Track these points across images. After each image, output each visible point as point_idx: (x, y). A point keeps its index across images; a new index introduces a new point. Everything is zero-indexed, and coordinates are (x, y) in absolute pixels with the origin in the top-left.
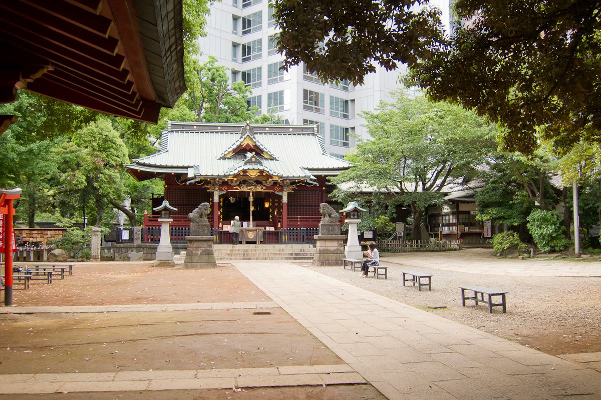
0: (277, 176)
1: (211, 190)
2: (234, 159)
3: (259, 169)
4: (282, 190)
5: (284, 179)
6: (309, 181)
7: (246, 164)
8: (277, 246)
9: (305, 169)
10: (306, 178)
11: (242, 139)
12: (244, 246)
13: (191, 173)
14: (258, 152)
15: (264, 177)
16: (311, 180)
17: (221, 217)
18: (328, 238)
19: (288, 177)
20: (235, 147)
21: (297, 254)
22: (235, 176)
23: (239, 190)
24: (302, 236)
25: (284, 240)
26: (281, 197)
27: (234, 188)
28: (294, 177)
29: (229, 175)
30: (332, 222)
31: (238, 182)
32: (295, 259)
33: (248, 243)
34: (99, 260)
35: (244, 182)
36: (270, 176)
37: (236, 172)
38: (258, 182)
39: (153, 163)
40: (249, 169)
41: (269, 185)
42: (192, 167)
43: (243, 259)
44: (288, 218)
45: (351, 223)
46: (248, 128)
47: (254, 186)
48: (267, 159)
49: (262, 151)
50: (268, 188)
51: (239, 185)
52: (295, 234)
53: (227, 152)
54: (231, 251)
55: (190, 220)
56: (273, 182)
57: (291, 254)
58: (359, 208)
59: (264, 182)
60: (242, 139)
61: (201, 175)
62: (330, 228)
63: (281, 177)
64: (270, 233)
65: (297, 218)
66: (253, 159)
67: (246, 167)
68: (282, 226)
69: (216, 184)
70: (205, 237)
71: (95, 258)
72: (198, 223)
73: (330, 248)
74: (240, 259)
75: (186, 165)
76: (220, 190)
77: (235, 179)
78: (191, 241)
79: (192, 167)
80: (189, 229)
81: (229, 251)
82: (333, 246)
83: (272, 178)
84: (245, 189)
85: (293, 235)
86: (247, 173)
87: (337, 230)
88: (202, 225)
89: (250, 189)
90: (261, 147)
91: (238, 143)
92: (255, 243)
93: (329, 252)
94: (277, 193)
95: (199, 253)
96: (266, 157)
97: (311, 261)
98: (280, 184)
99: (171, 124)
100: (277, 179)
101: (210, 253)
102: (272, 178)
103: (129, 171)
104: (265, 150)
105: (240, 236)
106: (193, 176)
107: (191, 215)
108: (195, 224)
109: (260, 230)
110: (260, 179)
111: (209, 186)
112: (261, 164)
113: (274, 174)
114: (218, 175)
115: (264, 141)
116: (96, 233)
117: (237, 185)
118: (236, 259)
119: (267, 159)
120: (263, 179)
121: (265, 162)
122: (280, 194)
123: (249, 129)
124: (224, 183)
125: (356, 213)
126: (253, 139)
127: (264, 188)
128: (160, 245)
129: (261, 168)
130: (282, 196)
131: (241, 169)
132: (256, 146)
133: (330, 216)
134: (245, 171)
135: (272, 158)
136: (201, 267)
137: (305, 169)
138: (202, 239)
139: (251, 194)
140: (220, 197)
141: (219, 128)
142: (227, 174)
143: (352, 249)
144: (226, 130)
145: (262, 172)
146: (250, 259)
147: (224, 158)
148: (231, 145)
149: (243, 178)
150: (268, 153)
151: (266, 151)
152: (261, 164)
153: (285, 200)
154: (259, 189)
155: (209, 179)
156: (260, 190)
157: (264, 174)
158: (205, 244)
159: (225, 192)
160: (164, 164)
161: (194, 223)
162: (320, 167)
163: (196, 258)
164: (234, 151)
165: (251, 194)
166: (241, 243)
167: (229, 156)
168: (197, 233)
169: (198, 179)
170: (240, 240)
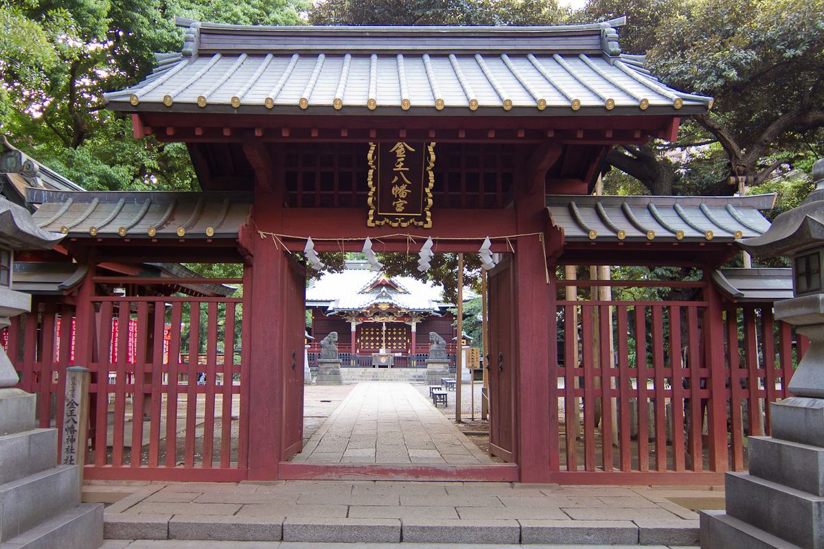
4: (411, 321)
7: (377, 298)
8: (404, 370)
12: (377, 370)
13: (331, 306)
16: (435, 311)
20: (372, 282)
21: (419, 377)
22: (368, 309)
29: (363, 308)
32: (417, 380)
33: (380, 367)
35: (377, 314)
36: (399, 309)
37: (369, 305)
38: (390, 314)
43: (372, 380)
50: (398, 319)
52: (422, 359)
54: (363, 373)
55: (321, 346)
57: (415, 376)
63: (408, 309)
64: (398, 358)
66: (384, 294)
67: (377, 301)
70: (333, 360)
73: (437, 370)
75: (328, 299)
76: (357, 320)
78: (322, 363)
82: (439, 368)
84: (378, 319)
91: (375, 279)
95: (328, 373)
96: (401, 291)
98: (408, 315)
101: (337, 373)
104: (399, 285)
105: (374, 361)
107: (322, 342)
112: (391, 298)
122: (409, 324)
124: (360, 314)
129: (390, 301)
131: (373, 302)
133: (437, 343)
134: (376, 305)
136: (329, 385)
139: (384, 324)
141: (362, 265)
145: (391, 305)
146: (377, 380)
147: (362, 292)
152: (391, 298)
153: (414, 329)
154: (390, 319)
156: (392, 321)
157: (394, 307)
158: (333, 365)
163: (325, 378)
164: (371, 286)
165: (384, 324)
166: (374, 367)
167: (367, 290)
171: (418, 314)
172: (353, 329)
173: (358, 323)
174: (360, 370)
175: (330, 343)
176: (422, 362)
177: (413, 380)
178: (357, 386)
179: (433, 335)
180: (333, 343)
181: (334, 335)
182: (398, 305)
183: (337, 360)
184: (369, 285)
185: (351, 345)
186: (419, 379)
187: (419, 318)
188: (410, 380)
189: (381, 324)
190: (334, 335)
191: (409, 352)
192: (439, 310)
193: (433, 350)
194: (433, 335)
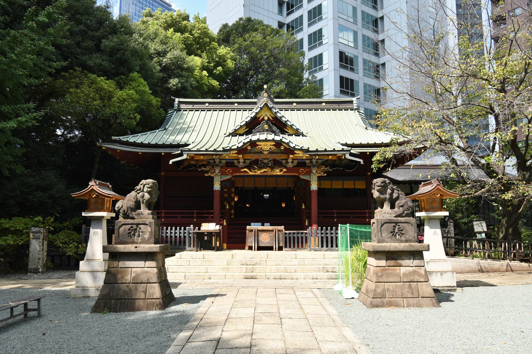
4: (309, 173)
6: (348, 156)
10: (345, 153)
17: (233, 212)
19: (317, 151)
27: (243, 170)
29: (231, 150)
31: (248, 162)
33: (260, 248)
38: (277, 164)
40: (259, 140)
41: (290, 165)
44: (319, 213)
45: (431, 219)
56: (296, 162)
59: (284, 162)
63: (307, 151)
65: (333, 213)
69: (217, 166)
71: (36, 271)
77: (241, 156)
81: (226, 264)
83: (293, 153)
89: (265, 172)
92: (270, 248)
94: (302, 177)
100: (300, 154)
102: (293, 153)
110: (278, 157)
111: (207, 169)
113: (297, 147)
114: (215, 150)
117: (246, 167)
127: (285, 170)
135: (298, 133)
147: (234, 134)
151: (290, 124)
154: (277, 172)
157: (282, 148)
159: (229, 177)
162: (364, 142)
167: (242, 131)
169: (185, 157)
171: (320, 161)
172: (217, 187)
184: (244, 123)
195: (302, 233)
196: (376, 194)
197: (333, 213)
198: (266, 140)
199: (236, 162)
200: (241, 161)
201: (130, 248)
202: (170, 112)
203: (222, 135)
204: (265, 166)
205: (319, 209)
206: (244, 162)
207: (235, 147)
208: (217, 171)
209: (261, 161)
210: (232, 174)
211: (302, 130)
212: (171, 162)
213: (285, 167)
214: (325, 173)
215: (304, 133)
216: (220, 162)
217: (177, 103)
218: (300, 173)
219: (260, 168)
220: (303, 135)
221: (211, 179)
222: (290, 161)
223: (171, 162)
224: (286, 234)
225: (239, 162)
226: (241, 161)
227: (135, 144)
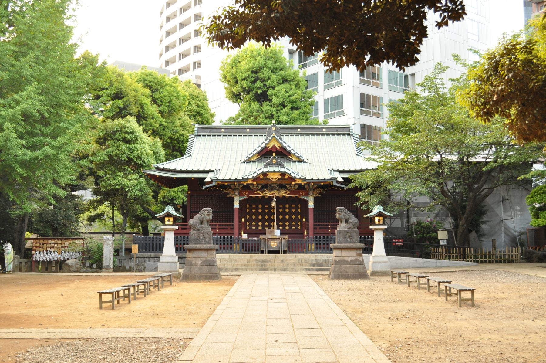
0: (300, 178)
1: (231, 195)
2: (260, 162)
3: (279, 171)
4: (307, 195)
5: (309, 182)
6: (335, 184)
7: (266, 166)
9: (334, 171)
11: (268, 141)
14: (284, 154)
15: (286, 181)
16: (337, 182)
18: (344, 247)
19: (312, 179)
20: (260, 149)
22: (254, 179)
23: (261, 194)
24: (148, 244)
25: (235, 249)
26: (307, 202)
28: (318, 179)
29: (248, 179)
30: (350, 228)
31: (260, 186)
33: (270, 252)
34: (112, 270)
36: (294, 179)
37: (255, 175)
39: (172, 168)
40: (268, 171)
41: (293, 189)
42: (213, 171)
43: (260, 270)
44: (315, 225)
45: (377, 229)
46: (274, 128)
47: (278, 190)
48: (295, 161)
49: (289, 153)
50: (292, 192)
51: (261, 189)
53: (252, 155)
54: (248, 261)
56: (297, 186)
57: (313, 265)
58: (384, 212)
59: (288, 186)
60: (268, 141)
61: (217, 179)
62: (348, 235)
63: (305, 179)
65: (328, 225)
66: (274, 161)
67: (265, 170)
68: (308, 234)
69: (236, 189)
70: (205, 246)
71: (108, 268)
72: (199, 230)
73: (346, 258)
74: (256, 270)
76: (241, 195)
77: (255, 183)
78: (190, 250)
79: (213, 171)
80: (188, 237)
81: (246, 261)
82: (350, 256)
84: (267, 194)
85: (320, 244)
86: (268, 177)
87: (356, 238)
88: (203, 233)
89: (273, 194)
90: (288, 148)
91: (264, 145)
92: (277, 252)
93: (346, 263)
94: (302, 198)
96: (294, 159)
97: (327, 273)
99: (198, 128)
100: (300, 182)
101: (211, 264)
103: (149, 177)
104: (292, 151)
105: (262, 245)
106: (210, 180)
107: (191, 222)
108: (195, 232)
109: (284, 238)
110: (283, 182)
111: (229, 191)
113: (297, 177)
114: (236, 179)
115: (291, 143)
116: (108, 242)
117: (259, 190)
118: (252, 270)
119: (295, 161)
120: (286, 183)
121: (287, 165)
122: (306, 198)
123: (276, 130)
125: (381, 218)
126: (280, 140)
127: (288, 192)
128: (163, 254)
129: (282, 170)
130: (308, 201)
132: (282, 148)
133: (347, 221)
134: (265, 174)
135: (300, 161)
137: (334, 171)
138: (202, 248)
139: (274, 199)
140: (241, 202)
142: (246, 177)
143: (377, 259)
144: (254, 133)
145: (283, 174)
147: (248, 161)
148: (256, 148)
149: (263, 181)
150: (296, 154)
152: (283, 166)
153: (311, 205)
154: (282, 193)
155: (226, 184)
156: (284, 195)
157: (286, 177)
158: (204, 254)
159: (245, 198)
160: (184, 169)
161: (194, 230)
162: (353, 168)
164: (259, 153)
166: (262, 252)
167: (254, 159)
168: (198, 240)
170: (262, 249)
171: (316, 186)
172: (236, 205)
173: (242, 198)
174: (246, 257)
175: (202, 223)
176: (324, 246)
177: (312, 270)
178: (240, 280)
179: (340, 211)
180: (205, 222)
181: (207, 212)
182: (293, 175)
183: (212, 245)
184: (256, 152)
185: (233, 225)
186: (319, 267)
187: (318, 190)
188: (309, 270)
189: (270, 199)
190: (207, 212)
191: (306, 233)
192: (342, 180)
193: (340, 232)
194: (340, 211)
195: (301, 241)
196: (337, 216)
197: (328, 225)
198: (274, 172)
199: (251, 186)
200: (255, 186)
201: (199, 246)
202: (190, 137)
203: (238, 160)
204: (273, 189)
205: (314, 222)
206: (257, 186)
207: (251, 177)
208: (237, 194)
209: (270, 185)
210: (248, 195)
211: (305, 158)
212: (204, 188)
213: (289, 190)
214: (319, 194)
215: (305, 160)
216: (239, 186)
217: (197, 129)
218: (300, 195)
219: (270, 191)
220: (305, 162)
221: (232, 200)
222: (292, 186)
223: (204, 188)
224: (289, 241)
225: (253, 186)
226: (255, 186)
227: (169, 171)
